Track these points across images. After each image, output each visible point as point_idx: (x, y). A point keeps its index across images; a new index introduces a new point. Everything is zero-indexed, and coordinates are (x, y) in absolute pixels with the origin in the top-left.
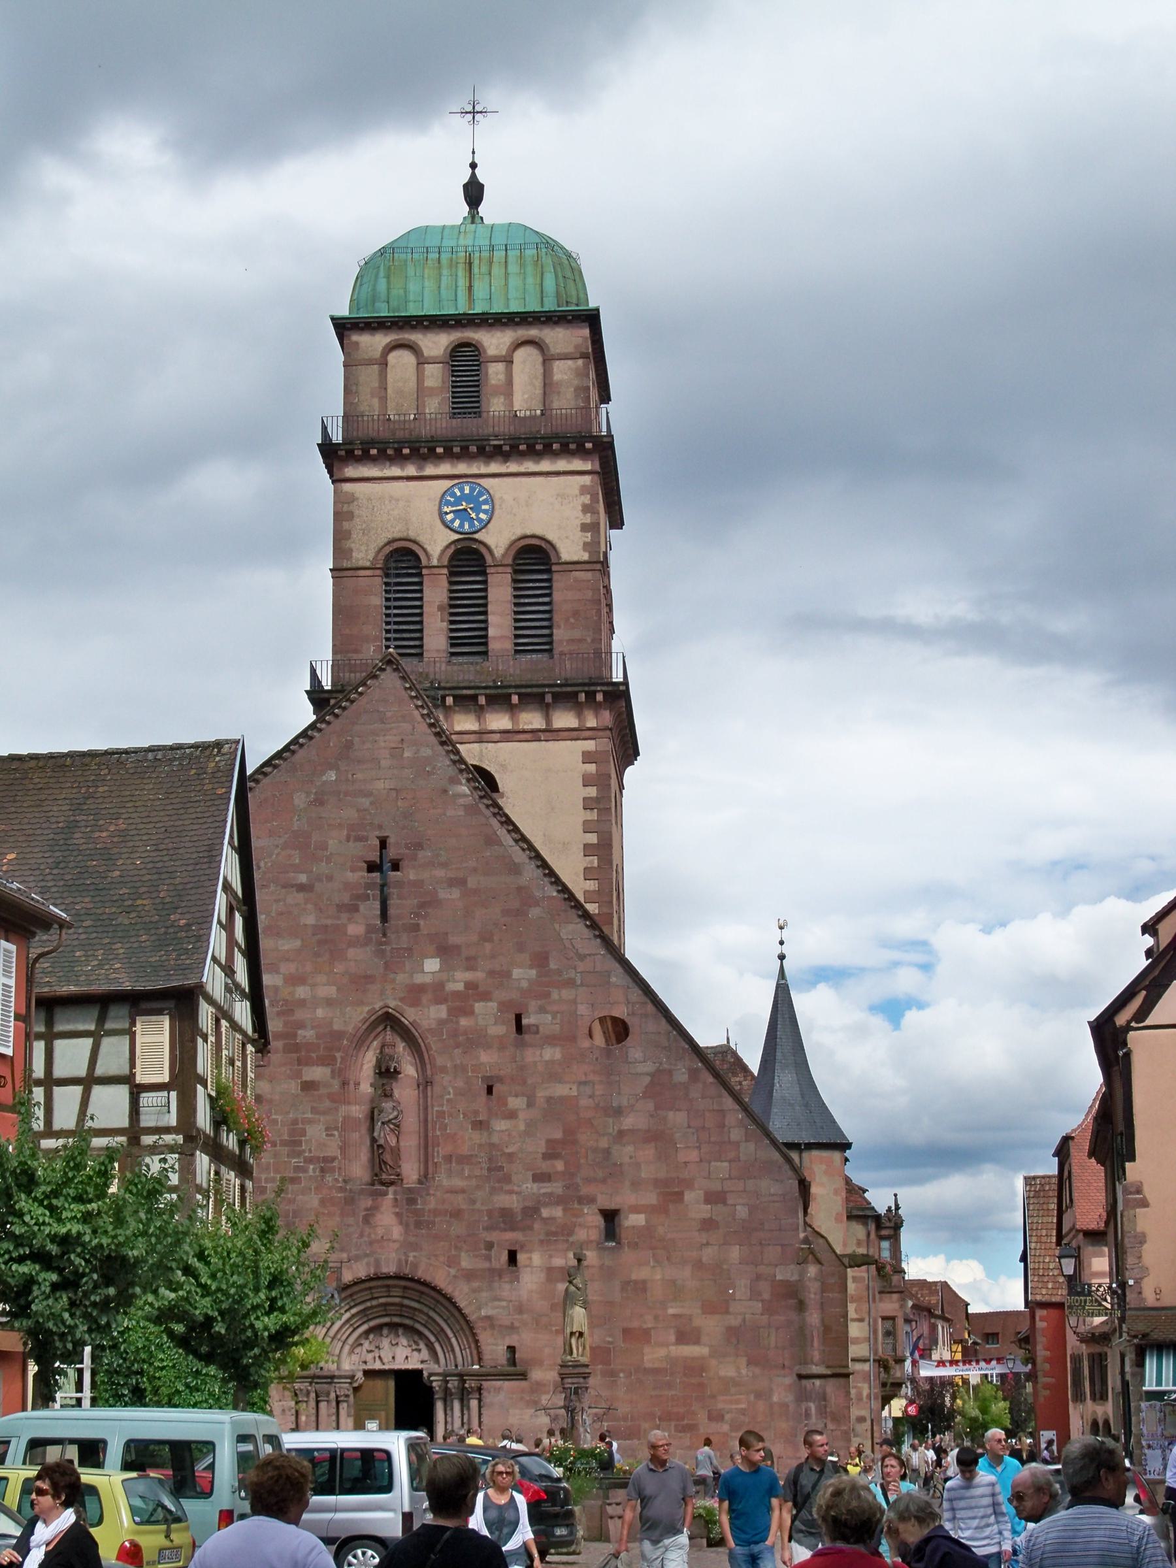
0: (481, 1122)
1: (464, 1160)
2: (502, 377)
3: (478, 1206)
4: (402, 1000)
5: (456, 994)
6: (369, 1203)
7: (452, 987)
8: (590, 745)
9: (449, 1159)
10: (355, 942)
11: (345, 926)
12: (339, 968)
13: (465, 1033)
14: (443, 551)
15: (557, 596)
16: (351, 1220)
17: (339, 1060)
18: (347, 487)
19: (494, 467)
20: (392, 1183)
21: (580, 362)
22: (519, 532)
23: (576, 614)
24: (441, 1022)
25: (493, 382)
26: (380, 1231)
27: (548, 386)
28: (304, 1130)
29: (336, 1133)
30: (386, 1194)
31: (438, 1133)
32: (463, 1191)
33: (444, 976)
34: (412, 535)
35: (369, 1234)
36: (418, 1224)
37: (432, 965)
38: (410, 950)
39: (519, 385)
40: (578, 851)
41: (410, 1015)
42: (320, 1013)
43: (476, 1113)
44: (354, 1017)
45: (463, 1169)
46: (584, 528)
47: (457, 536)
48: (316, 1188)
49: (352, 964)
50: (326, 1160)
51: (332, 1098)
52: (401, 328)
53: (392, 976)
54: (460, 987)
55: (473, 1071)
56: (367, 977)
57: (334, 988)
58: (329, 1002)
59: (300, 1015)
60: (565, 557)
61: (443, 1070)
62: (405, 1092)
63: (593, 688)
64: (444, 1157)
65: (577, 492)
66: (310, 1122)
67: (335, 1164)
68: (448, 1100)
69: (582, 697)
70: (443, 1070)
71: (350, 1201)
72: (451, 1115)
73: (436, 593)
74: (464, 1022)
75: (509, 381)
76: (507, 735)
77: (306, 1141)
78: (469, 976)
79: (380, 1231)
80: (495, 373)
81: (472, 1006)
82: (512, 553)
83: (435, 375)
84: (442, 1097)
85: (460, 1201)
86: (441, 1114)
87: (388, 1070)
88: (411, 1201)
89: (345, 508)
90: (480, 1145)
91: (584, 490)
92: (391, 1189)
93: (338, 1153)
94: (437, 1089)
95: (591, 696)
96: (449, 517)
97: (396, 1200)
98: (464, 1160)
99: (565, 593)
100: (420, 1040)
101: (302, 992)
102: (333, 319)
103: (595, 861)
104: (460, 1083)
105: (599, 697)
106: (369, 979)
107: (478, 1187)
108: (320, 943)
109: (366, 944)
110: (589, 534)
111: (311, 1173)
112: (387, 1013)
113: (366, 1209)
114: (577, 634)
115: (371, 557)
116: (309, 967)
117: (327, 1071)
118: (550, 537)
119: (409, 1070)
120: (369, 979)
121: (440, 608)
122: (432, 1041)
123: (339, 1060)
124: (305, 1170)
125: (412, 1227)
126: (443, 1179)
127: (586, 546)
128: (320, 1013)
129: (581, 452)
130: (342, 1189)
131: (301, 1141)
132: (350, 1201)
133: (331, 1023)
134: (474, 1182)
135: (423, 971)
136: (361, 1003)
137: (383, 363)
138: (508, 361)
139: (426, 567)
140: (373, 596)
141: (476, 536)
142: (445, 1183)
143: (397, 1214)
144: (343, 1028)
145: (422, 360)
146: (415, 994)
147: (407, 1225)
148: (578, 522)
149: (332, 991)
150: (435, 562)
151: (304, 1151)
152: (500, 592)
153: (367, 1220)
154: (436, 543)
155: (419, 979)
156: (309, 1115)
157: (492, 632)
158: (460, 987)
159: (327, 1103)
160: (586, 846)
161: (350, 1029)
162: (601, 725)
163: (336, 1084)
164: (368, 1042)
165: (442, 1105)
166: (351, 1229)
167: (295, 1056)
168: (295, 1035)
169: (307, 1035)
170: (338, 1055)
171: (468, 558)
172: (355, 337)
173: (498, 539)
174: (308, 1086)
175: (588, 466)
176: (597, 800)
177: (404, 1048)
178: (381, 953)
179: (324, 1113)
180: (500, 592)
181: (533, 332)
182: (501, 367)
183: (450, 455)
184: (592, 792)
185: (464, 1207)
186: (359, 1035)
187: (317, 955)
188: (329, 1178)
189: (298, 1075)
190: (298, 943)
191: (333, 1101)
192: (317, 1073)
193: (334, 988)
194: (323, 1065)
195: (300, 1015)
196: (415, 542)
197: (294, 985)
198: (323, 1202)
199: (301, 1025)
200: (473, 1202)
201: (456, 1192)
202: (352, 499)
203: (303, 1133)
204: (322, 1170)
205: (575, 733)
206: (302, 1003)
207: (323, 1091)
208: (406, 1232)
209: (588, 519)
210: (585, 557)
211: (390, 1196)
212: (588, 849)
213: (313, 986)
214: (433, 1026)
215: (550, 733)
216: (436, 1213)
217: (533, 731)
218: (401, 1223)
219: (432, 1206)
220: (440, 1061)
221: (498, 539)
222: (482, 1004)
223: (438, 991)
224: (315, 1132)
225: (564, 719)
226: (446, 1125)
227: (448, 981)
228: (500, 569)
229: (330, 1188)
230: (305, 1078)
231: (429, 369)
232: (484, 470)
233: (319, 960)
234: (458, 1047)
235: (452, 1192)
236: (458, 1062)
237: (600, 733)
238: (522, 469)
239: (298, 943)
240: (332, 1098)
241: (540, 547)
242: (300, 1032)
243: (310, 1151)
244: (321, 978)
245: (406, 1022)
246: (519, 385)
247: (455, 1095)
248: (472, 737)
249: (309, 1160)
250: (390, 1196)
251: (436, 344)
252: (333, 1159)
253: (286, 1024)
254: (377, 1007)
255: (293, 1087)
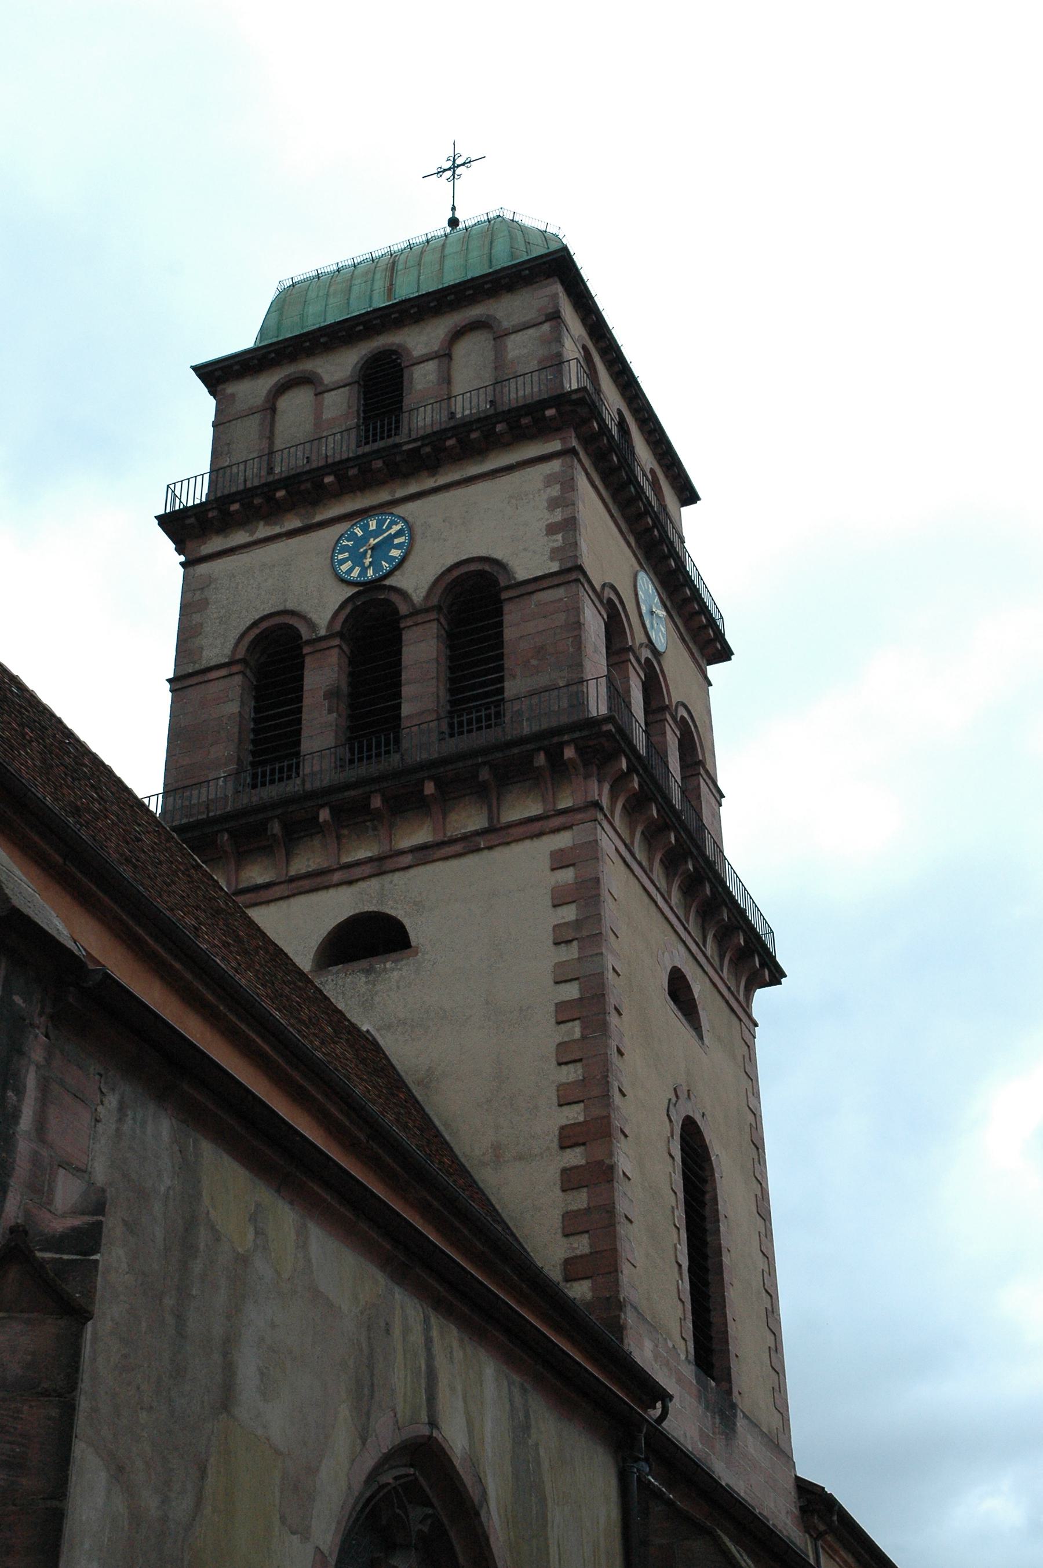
2: (433, 377)
8: (563, 840)
14: (336, 614)
15: (509, 634)
18: (203, 569)
19: (413, 488)
21: (546, 327)
22: (450, 561)
23: (540, 651)
25: (419, 387)
27: (499, 362)
34: (290, 606)
39: (454, 378)
40: (546, 1015)
46: (552, 529)
47: (350, 591)
52: (293, 358)
60: (522, 572)
63: (555, 740)
65: (541, 485)
69: (541, 760)
73: (322, 676)
75: (447, 380)
76: (424, 854)
80: (422, 378)
82: (439, 590)
83: (339, 405)
89: (198, 596)
91: (549, 481)
95: (555, 757)
96: (345, 567)
99: (520, 626)
102: (196, 369)
103: (575, 1030)
105: (569, 753)
110: (559, 537)
114: (542, 681)
115: (227, 651)
118: (498, 555)
121: (332, 694)
127: (555, 554)
129: (541, 429)
137: (270, 408)
138: (445, 355)
139: (309, 642)
140: (229, 702)
141: (387, 582)
145: (320, 389)
148: (543, 525)
150: (323, 632)
152: (422, 652)
154: (322, 603)
157: (406, 710)
160: (560, 1006)
162: (580, 802)
171: (373, 620)
172: (231, 388)
173: (416, 582)
175: (556, 446)
176: (578, 924)
180: (422, 652)
181: (476, 312)
182: (431, 366)
183: (346, 487)
184: (569, 913)
196: (293, 613)
202: (209, 581)
205: (537, 826)
209: (558, 516)
210: (555, 567)
212: (564, 1013)
215: (496, 835)
217: (465, 838)
221: (416, 582)
225: (520, 807)
228: (420, 619)
231: (329, 398)
232: (400, 493)
237: (579, 816)
238: (456, 476)
241: (482, 573)
246: (454, 378)
248: (367, 870)
251: (340, 366)
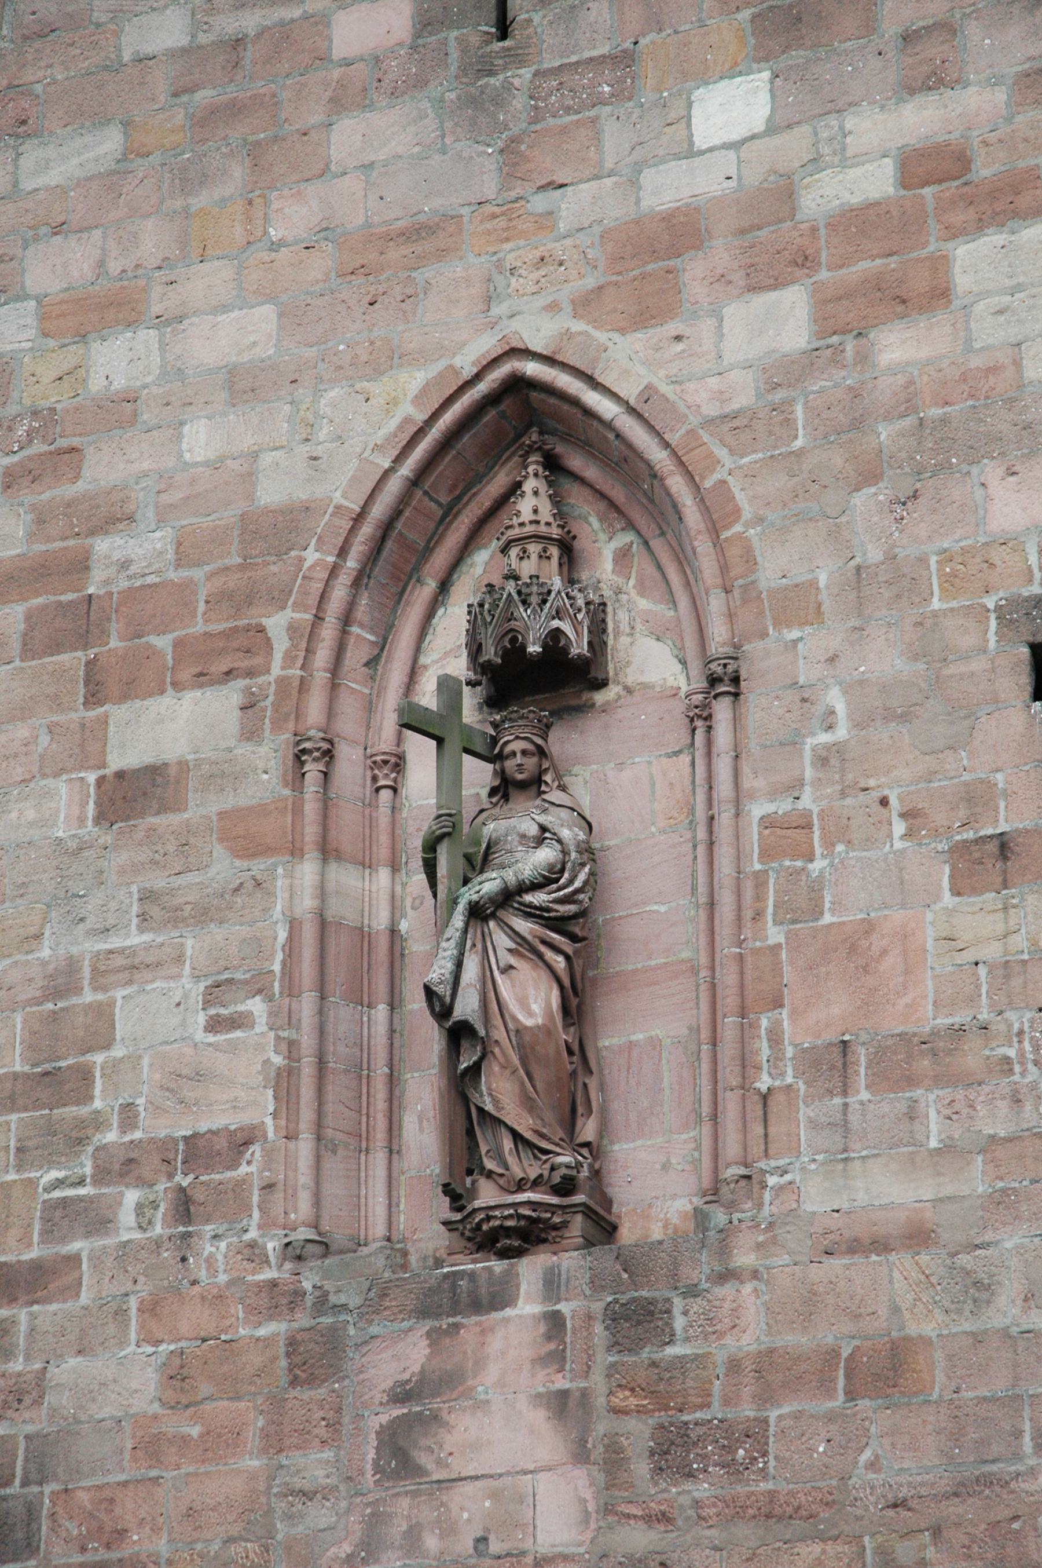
0: (1004, 846)
1: (918, 1059)
3: (1006, 1311)
4: (584, 305)
5: (858, 223)
6: (400, 1353)
7: (826, 194)
9: (834, 1063)
10: (364, 86)
11: (321, 21)
12: (292, 216)
13: (908, 403)
16: (314, 1465)
17: (281, 644)
20: (527, 1235)
24: (783, 375)
26: (470, 1508)
28: (103, 1013)
29: (256, 1006)
30: (499, 1297)
31: (775, 935)
32: (918, 1236)
33: (795, 146)
35: (413, 1536)
36: (673, 1452)
37: (732, 109)
38: (624, 60)
41: (625, 369)
42: (200, 440)
43: (977, 797)
44: (353, 437)
45: (912, 1114)
48: (151, 1309)
49: (352, 183)
50: (197, 1151)
51: (244, 836)
53: (539, 203)
54: (875, 181)
55: (951, 584)
56: (418, 232)
57: (266, 314)
58: (243, 385)
59: (103, 469)
61: (798, 605)
62: (622, 777)
64: (812, 1062)
66: (134, 967)
67: (250, 1167)
68: (822, 760)
70: (798, 605)
71: (315, 1359)
72: (839, 832)
74: (900, 347)
77: (112, 1068)
78: (921, 120)
79: (470, 1508)
81: (941, 263)
84: (793, 743)
85: (899, 1293)
86: (790, 834)
87: (515, 651)
88: (636, 1321)
90: (1005, 969)
92: (530, 1270)
93: (261, 1110)
94: (762, 706)
97: (555, 1322)
98: (918, 1059)
100: (676, 484)
101: (117, 361)
104: (885, 659)
106: (425, 236)
107: (1001, 1201)
108: (206, 121)
109: (420, 83)
111: (127, 1226)
112: (517, 384)
113: (402, 1394)
116: (152, 240)
117: (223, 702)
119: (649, 661)
120: (425, 236)
122: (726, 466)
123: (281, 644)
124: (96, 1219)
125: (641, 1468)
126: (813, 1187)
128: (200, 440)
130: (279, 1299)
131: (85, 1075)
132: (315, 1359)
133: (249, 478)
134: (976, 1180)
135: (690, 152)
136: (385, 359)
142: (817, 1198)
143: (560, 1404)
144: (302, 495)
146: (650, 265)
147: (614, 1462)
149: (248, 332)
151: (98, 1122)
153: (399, 1456)
155: (667, 188)
156: (136, 939)
158: (875, 181)
159: (222, 867)
161: (340, 487)
163: (268, 756)
164: (441, 558)
165: (794, 787)
166: (319, 1516)
167: (73, 660)
168: (80, 565)
169: (132, 554)
170: (277, 624)
174: (131, 796)
177: (622, 557)
178: (478, 107)
179: (203, 915)
185: (924, 1326)
186: (379, 511)
187: (188, 181)
188: (215, 1250)
189: (89, 744)
190: (110, 143)
191: (248, 847)
192: (174, 725)
193: (266, 314)
194: (202, 679)
195: (103, 469)
197: (82, 337)
198: (177, 1375)
199: (115, 517)
200: (980, 1290)
201: (880, 1245)
203: (100, 1030)
204: (185, 1208)
206: (121, 411)
207: (201, 807)
208: (608, 1509)
211: (528, 1306)
213: (170, 321)
214: (743, 399)
216: (771, 1373)
218: (581, 1455)
219: (749, 1339)
220: (775, 566)
222: (994, 239)
223: (770, 238)
224: (156, 1020)
226: (816, 889)
227: (816, 163)
229: (218, 1299)
230: (116, 762)
233: (198, 201)
234: (870, 476)
235: (854, 1247)
236: (874, 555)
239: (110, 143)
240: (244, 836)
242: (102, 545)
243: (128, 1115)
244: (211, 279)
245: (606, 408)
247: (858, 725)
249: (123, 1167)
250: (528, 1306)
252: (242, 1141)
253: (41, 519)
254: (466, 363)
255: (64, 806)
